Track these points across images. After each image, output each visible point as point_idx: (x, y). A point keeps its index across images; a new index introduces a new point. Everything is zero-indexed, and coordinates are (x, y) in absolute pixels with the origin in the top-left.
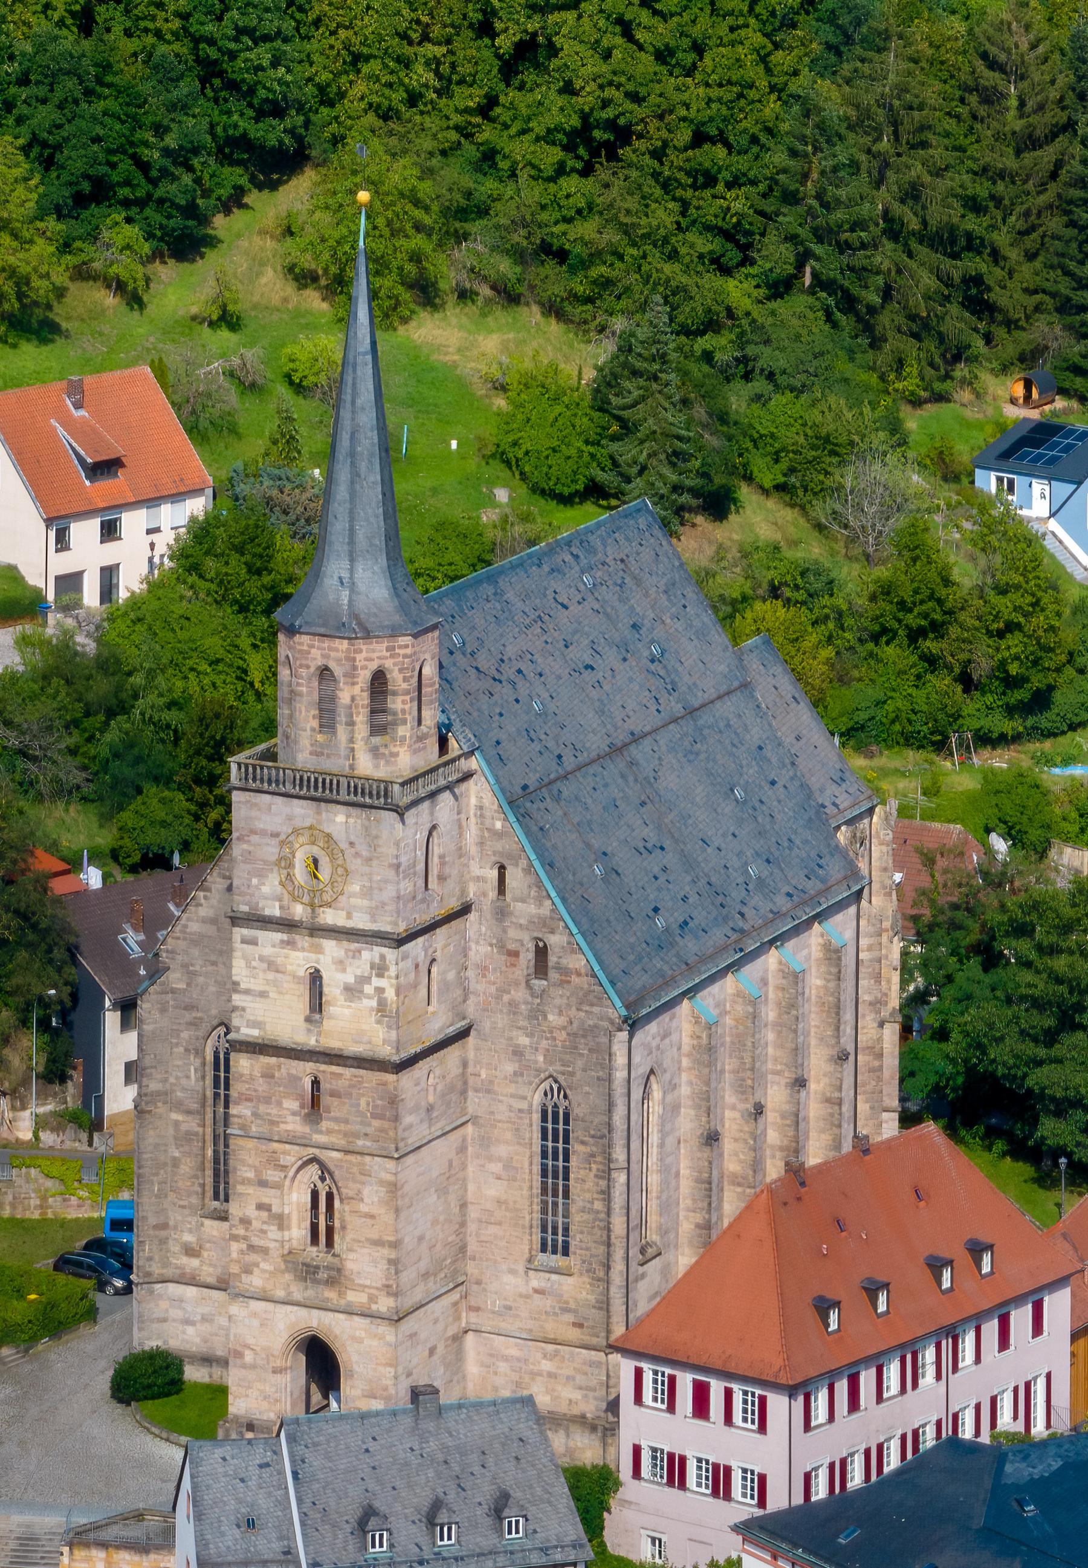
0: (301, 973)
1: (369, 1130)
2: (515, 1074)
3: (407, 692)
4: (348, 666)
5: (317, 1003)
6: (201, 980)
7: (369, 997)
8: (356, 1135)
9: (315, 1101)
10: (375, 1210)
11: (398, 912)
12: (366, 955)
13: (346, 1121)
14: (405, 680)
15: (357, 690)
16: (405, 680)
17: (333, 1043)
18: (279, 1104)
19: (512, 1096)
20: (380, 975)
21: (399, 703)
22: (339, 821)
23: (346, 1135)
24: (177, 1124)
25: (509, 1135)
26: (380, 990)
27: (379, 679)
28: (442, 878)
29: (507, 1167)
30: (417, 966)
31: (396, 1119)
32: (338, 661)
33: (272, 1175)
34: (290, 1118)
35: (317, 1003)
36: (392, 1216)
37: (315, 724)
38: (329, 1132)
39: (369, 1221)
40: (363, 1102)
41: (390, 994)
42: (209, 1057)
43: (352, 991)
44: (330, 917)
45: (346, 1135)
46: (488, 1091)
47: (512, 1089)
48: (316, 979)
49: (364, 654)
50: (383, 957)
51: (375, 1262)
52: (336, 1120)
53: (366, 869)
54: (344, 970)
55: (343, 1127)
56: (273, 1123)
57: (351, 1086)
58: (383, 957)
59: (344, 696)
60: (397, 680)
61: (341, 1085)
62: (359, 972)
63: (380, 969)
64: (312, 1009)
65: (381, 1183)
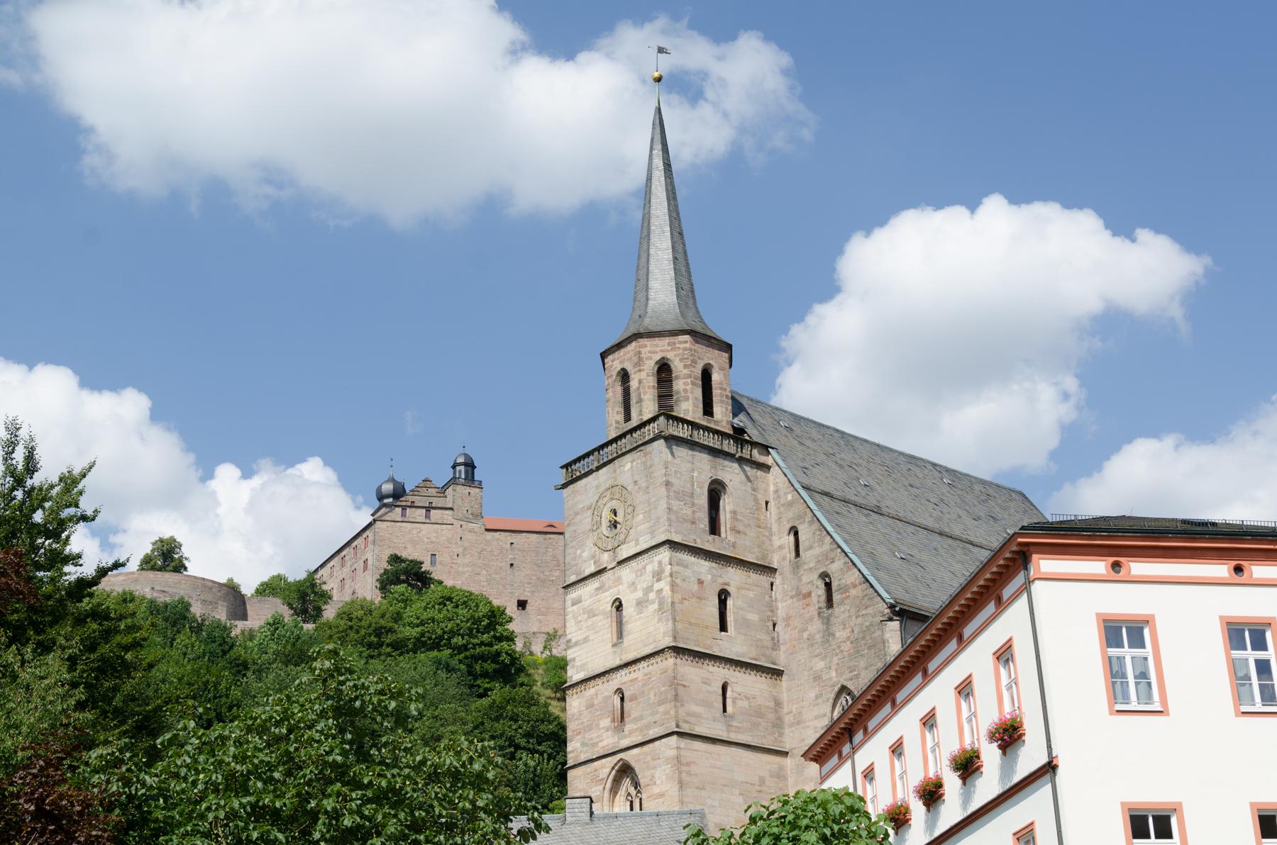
0: (608, 607)
1: (657, 717)
2: (817, 698)
4: (635, 359)
7: (653, 602)
8: (648, 727)
11: (669, 519)
12: (649, 568)
13: (641, 718)
14: (685, 366)
15: (643, 375)
16: (685, 366)
19: (817, 718)
20: (659, 580)
21: (679, 385)
22: (627, 468)
23: (641, 730)
26: (660, 591)
27: (664, 371)
30: (700, 582)
32: (630, 359)
34: (605, 735)
36: (676, 788)
38: (631, 733)
39: (661, 800)
41: (667, 591)
43: (640, 603)
44: (625, 552)
46: (798, 723)
48: (618, 605)
49: (648, 349)
52: (636, 720)
53: (646, 497)
54: (635, 589)
55: (639, 724)
56: (595, 744)
57: (644, 685)
58: (660, 563)
59: (634, 384)
60: (677, 366)
62: (645, 585)
63: (658, 576)
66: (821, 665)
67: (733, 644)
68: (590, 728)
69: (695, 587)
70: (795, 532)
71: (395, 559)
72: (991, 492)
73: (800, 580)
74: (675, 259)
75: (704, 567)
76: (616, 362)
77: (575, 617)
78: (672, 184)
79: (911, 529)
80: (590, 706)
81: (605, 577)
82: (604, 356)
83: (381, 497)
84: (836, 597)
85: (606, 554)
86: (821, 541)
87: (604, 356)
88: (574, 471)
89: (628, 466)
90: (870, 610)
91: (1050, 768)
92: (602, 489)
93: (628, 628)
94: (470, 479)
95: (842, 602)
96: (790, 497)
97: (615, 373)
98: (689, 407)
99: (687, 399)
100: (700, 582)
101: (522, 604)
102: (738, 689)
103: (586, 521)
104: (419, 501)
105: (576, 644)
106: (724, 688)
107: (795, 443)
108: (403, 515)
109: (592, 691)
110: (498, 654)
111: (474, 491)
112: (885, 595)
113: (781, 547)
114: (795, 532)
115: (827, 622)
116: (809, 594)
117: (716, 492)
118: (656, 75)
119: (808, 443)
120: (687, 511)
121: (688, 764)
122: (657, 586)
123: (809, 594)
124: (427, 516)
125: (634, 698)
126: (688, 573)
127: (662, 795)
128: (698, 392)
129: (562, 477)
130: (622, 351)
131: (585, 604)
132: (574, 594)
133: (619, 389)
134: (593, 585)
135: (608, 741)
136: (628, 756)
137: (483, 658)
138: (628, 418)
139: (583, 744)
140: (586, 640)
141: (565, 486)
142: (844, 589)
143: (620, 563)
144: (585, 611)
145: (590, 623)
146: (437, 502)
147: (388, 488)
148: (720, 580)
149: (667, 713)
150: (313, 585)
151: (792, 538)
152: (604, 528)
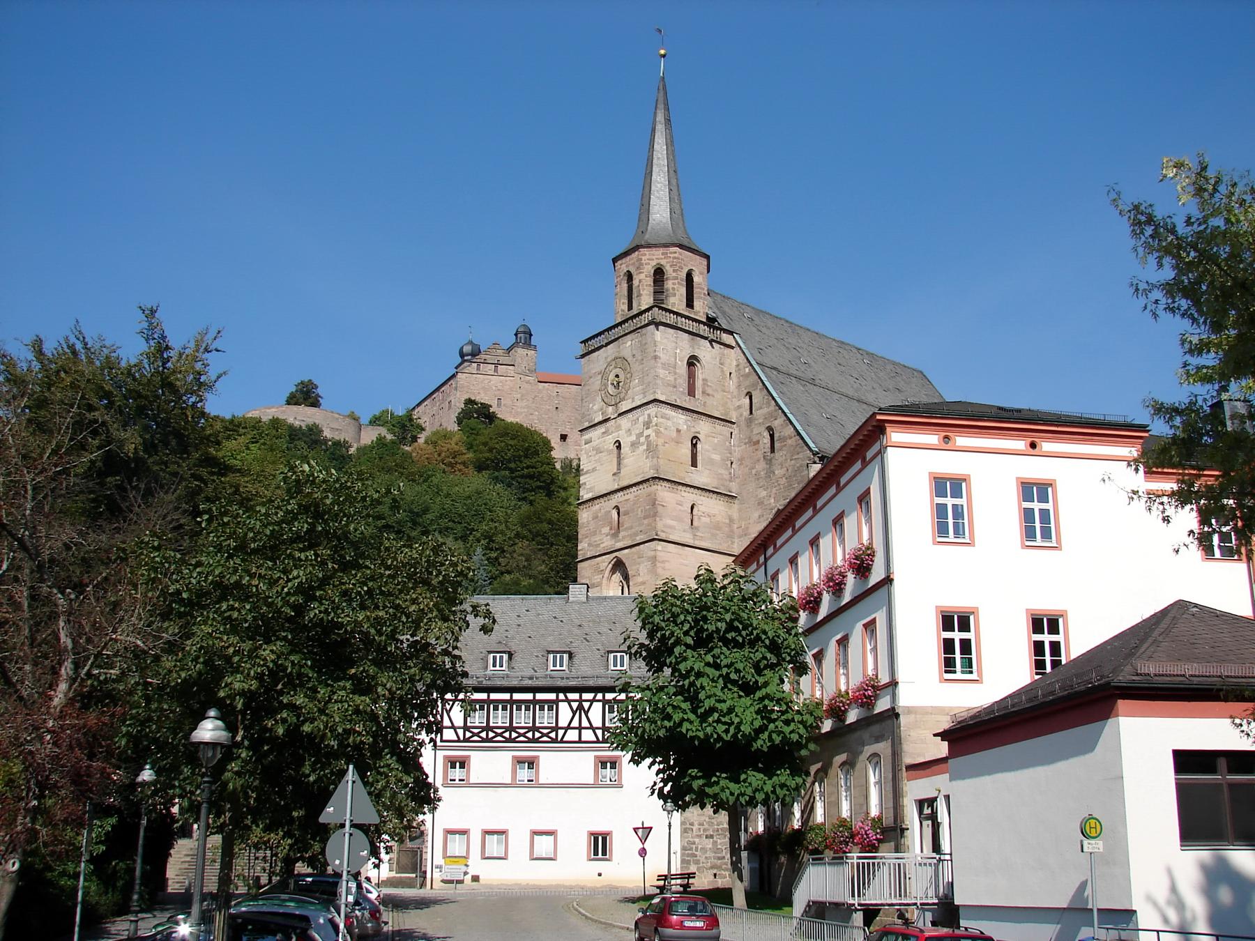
0: (612, 447)
12: (641, 419)
13: (631, 528)
15: (642, 276)
21: (669, 285)
23: (630, 536)
30: (678, 431)
43: (634, 445)
44: (625, 406)
52: (626, 529)
55: (630, 532)
59: (635, 283)
60: (669, 270)
63: (647, 425)
66: (764, 493)
67: (701, 477)
68: (595, 533)
69: (674, 434)
71: (469, 402)
72: (899, 371)
74: (670, 190)
75: (680, 419)
76: (623, 266)
77: (587, 453)
78: (672, 136)
79: (836, 396)
82: (615, 260)
83: (462, 355)
84: (777, 445)
86: (768, 403)
87: (615, 260)
88: (592, 344)
90: (801, 456)
91: (888, 581)
93: (625, 462)
94: (528, 344)
95: (781, 450)
98: (677, 300)
100: (678, 431)
101: (564, 437)
102: (702, 508)
103: (597, 382)
104: (489, 358)
105: (587, 472)
106: (692, 508)
107: (754, 329)
108: (478, 369)
110: (541, 474)
111: (531, 353)
112: (812, 445)
113: (739, 407)
115: (769, 462)
117: (692, 362)
118: (662, 52)
119: (764, 330)
120: (670, 378)
121: (663, 562)
122: (646, 433)
124: (496, 370)
125: (626, 513)
126: (669, 423)
127: (643, 583)
128: (683, 290)
129: (581, 349)
132: (587, 436)
133: (625, 286)
134: (600, 430)
135: (608, 543)
137: (531, 477)
138: (630, 307)
139: (590, 545)
140: (594, 470)
141: (583, 356)
142: (783, 439)
143: (620, 415)
146: (502, 360)
147: (467, 349)
148: (693, 430)
150: (411, 420)
151: (748, 400)
152: (611, 389)
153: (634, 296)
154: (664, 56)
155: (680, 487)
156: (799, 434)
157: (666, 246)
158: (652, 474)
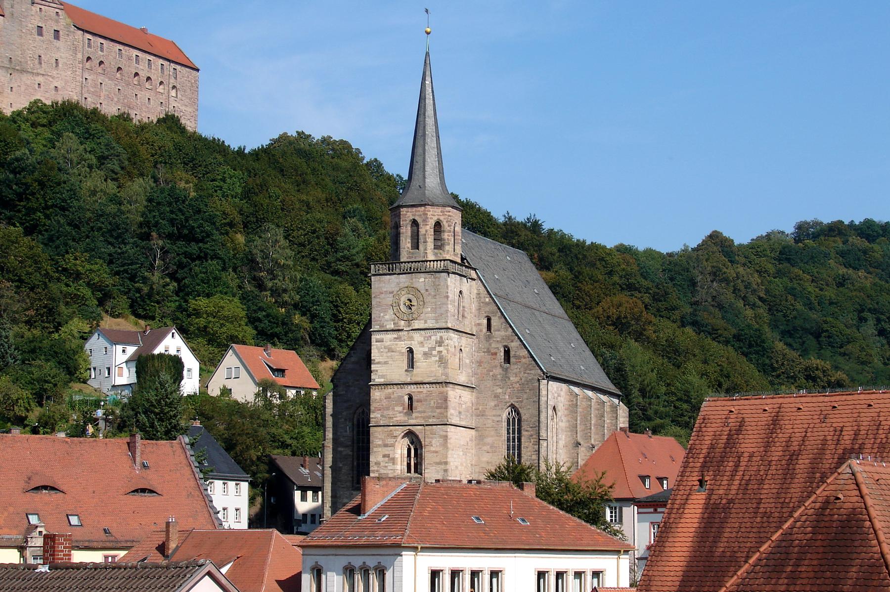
0: (405, 350)
1: (435, 414)
3: (450, 231)
5: (411, 364)
6: (352, 388)
7: (435, 356)
9: (411, 407)
10: (438, 449)
12: (433, 338)
13: (424, 412)
14: (449, 226)
15: (428, 227)
16: (449, 226)
17: (419, 379)
18: (393, 409)
21: (445, 236)
22: (421, 281)
24: (341, 452)
25: (493, 433)
26: (440, 352)
27: (438, 225)
28: (463, 316)
29: (491, 447)
31: (446, 408)
33: (390, 441)
34: (398, 415)
35: (411, 364)
37: (409, 245)
38: (417, 418)
40: (432, 402)
42: (355, 422)
44: (417, 325)
45: (424, 418)
47: (494, 413)
48: (411, 351)
50: (441, 337)
51: (438, 472)
52: (419, 412)
53: (434, 300)
55: (423, 415)
56: (390, 418)
58: (441, 337)
59: (422, 231)
60: (445, 224)
61: (421, 396)
63: (440, 343)
64: (409, 367)
65: (441, 437)
66: (500, 391)
68: (388, 409)
70: (489, 320)
73: (490, 345)
77: (377, 348)
80: (388, 397)
81: (400, 333)
85: (403, 322)
89: (422, 280)
92: (402, 285)
95: (516, 363)
96: (487, 300)
97: (408, 220)
99: (449, 244)
105: (379, 363)
109: (390, 391)
113: (479, 324)
114: (489, 320)
116: (496, 354)
118: (429, 30)
123: (496, 354)
127: (437, 452)
130: (414, 209)
131: (389, 343)
135: (400, 418)
136: (415, 429)
140: (386, 363)
142: (518, 357)
144: (385, 348)
145: (389, 354)
149: (441, 413)
151: (485, 321)
153: (421, 240)
154: (428, 33)
155: (456, 387)
156: (532, 357)
157: (444, 206)
158: (442, 379)
